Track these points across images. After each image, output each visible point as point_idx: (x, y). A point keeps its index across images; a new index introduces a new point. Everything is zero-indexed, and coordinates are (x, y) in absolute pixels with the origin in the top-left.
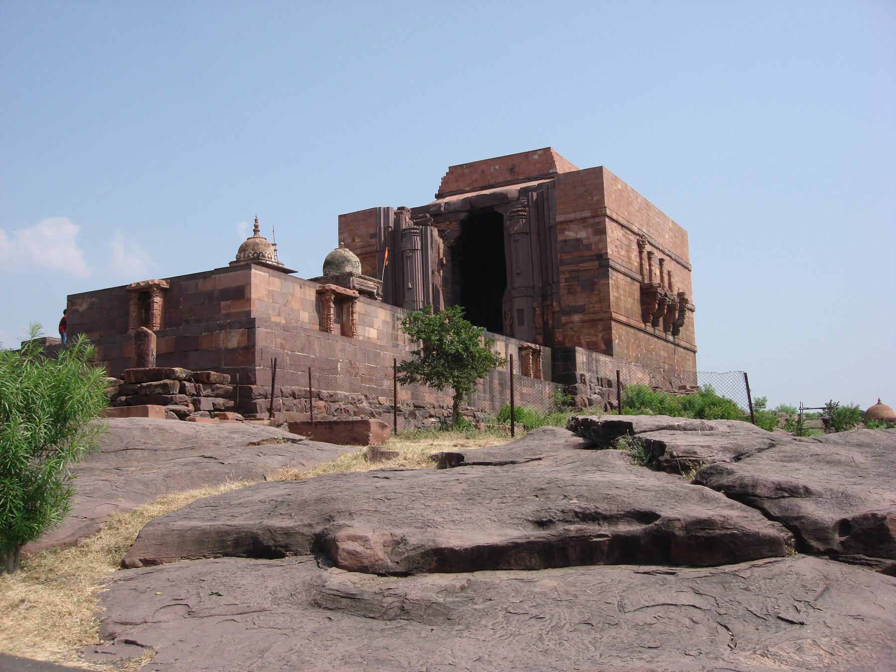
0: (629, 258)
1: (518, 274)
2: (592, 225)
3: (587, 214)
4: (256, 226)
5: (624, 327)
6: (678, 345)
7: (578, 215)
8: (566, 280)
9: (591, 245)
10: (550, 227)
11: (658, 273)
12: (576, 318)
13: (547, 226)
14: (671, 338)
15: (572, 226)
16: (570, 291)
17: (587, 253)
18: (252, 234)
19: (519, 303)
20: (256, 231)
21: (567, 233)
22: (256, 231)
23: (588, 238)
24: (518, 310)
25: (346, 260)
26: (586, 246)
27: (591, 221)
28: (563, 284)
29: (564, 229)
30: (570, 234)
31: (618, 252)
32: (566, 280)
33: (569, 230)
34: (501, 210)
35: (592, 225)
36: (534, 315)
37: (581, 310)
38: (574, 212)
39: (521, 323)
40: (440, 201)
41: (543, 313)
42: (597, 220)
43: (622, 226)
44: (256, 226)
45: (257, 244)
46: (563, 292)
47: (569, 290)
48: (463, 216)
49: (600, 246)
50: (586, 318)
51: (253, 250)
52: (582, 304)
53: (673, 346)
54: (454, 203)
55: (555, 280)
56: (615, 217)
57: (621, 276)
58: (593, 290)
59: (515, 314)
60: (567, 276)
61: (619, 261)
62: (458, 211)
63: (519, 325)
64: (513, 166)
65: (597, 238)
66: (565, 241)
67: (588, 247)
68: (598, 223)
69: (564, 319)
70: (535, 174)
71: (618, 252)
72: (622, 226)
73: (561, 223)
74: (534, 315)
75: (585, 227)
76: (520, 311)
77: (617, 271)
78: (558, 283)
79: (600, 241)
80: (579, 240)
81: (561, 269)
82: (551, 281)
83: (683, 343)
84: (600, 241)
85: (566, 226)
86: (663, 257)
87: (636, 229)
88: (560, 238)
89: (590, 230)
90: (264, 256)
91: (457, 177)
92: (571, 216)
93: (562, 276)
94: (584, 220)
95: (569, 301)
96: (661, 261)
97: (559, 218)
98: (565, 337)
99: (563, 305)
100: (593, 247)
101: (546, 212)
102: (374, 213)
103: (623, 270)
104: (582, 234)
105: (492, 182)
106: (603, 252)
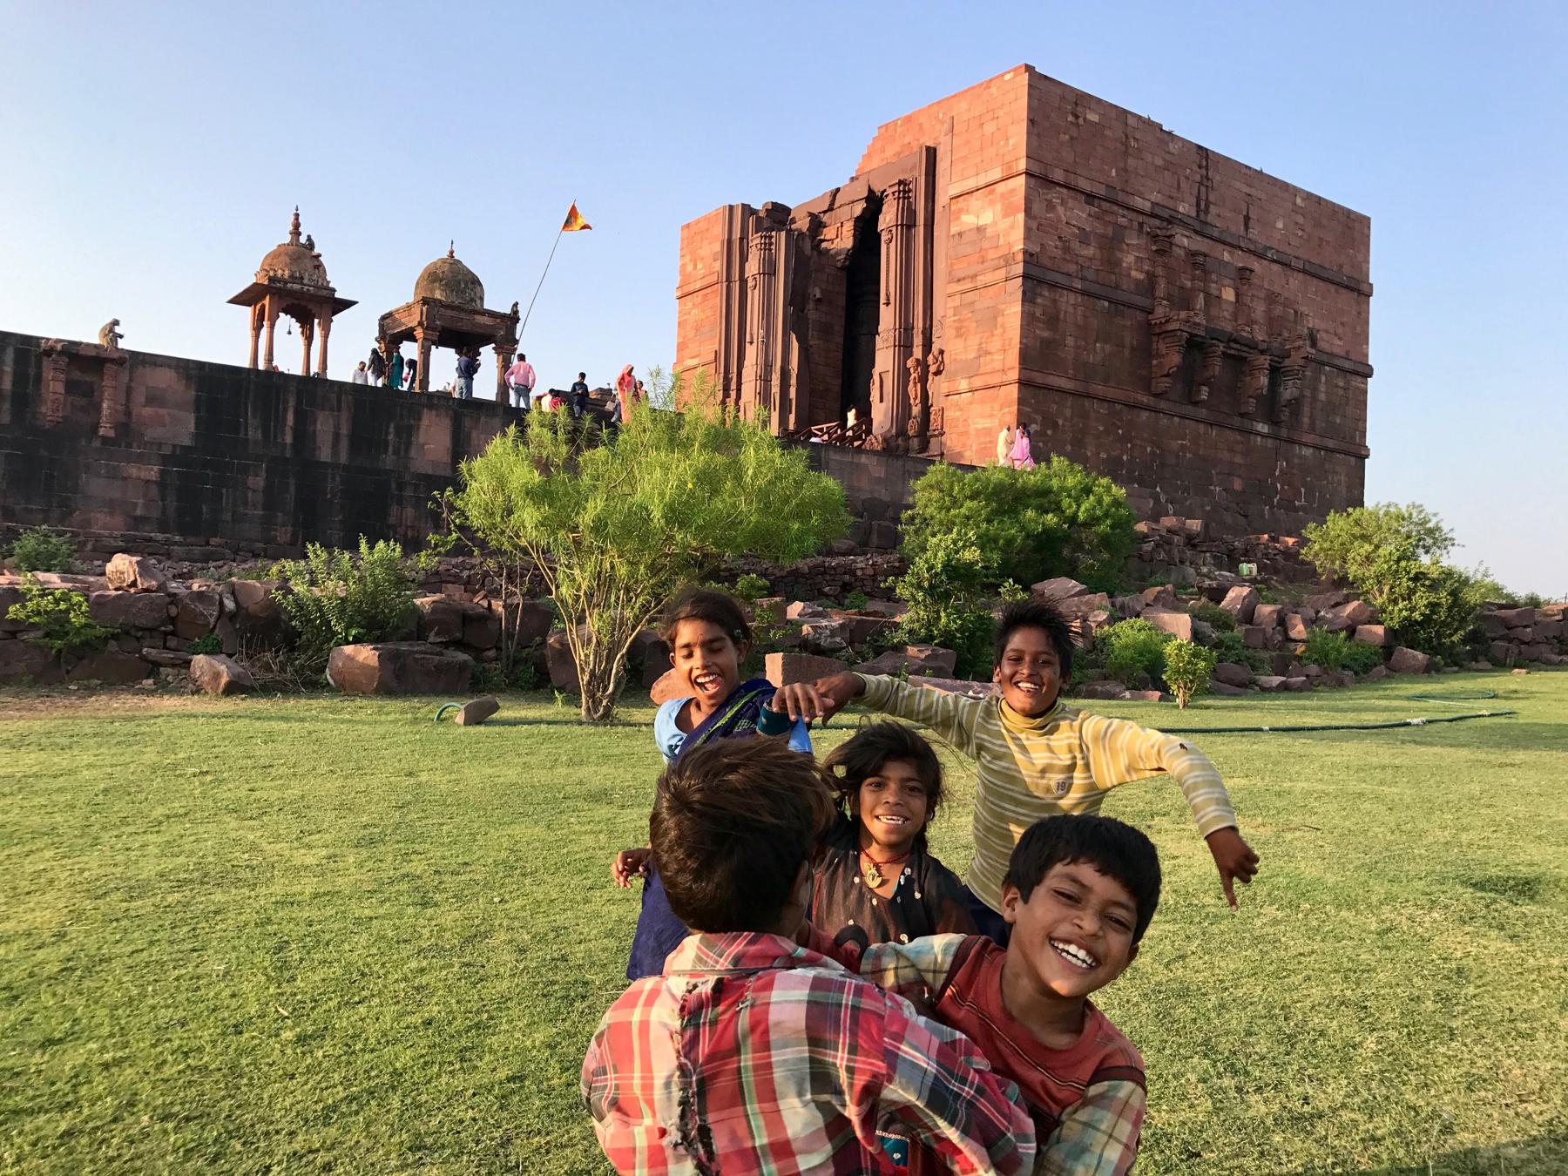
0: (1113, 264)
3: (996, 174)
4: (297, 226)
5: (1070, 401)
6: (1292, 441)
11: (1229, 295)
14: (1263, 428)
15: (975, 202)
18: (287, 239)
20: (296, 232)
21: (964, 218)
22: (296, 232)
23: (995, 223)
27: (1001, 188)
29: (960, 211)
30: (969, 220)
31: (1067, 250)
35: (1002, 195)
43: (1090, 198)
44: (297, 226)
47: (958, 329)
50: (978, 382)
53: (1270, 443)
56: (1058, 175)
57: (1072, 298)
61: (1072, 268)
71: (1067, 250)
72: (1090, 198)
75: (992, 203)
77: (1054, 286)
80: (980, 229)
83: (1307, 438)
86: (1256, 265)
87: (1147, 206)
88: (954, 229)
89: (999, 206)
92: (971, 184)
96: (1243, 275)
100: (1001, 241)
103: (1078, 285)
104: (986, 218)
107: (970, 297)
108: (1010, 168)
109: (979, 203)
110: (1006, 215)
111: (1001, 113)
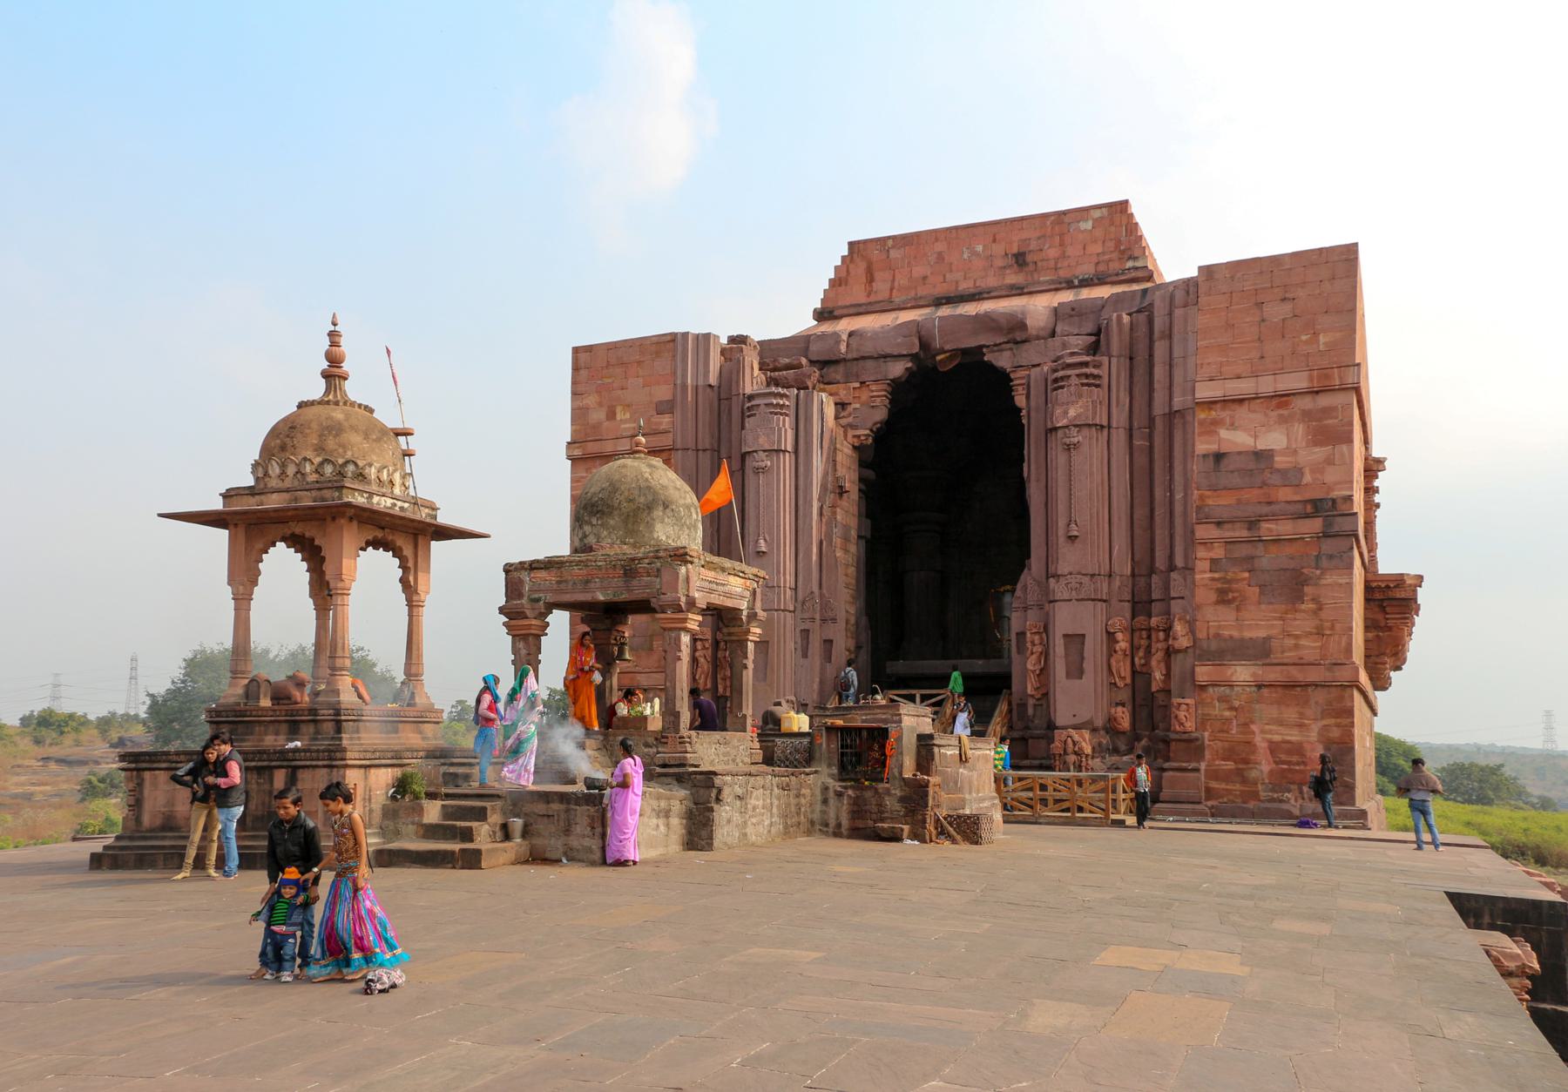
1: (1072, 539)
2: (1307, 415)
3: (1297, 381)
7: (1267, 385)
8: (1215, 564)
9: (1300, 471)
10: (1171, 415)
12: (1242, 673)
13: (1159, 408)
15: (1242, 412)
16: (1224, 597)
17: (1285, 494)
19: (1065, 619)
21: (1224, 433)
24: (1065, 636)
25: (650, 503)
26: (1283, 473)
27: (1306, 403)
28: (1203, 575)
29: (1216, 423)
30: (1236, 438)
32: (1215, 564)
33: (1232, 427)
34: (1003, 361)
35: (1307, 415)
36: (1111, 652)
37: (1259, 651)
38: (1255, 375)
39: (1075, 671)
40: (827, 328)
41: (1134, 649)
42: (1324, 401)
45: (336, 429)
46: (1205, 595)
47: (1222, 592)
48: (898, 369)
49: (1331, 476)
51: (320, 449)
52: (1262, 634)
54: (875, 335)
55: (1179, 562)
58: (1300, 598)
59: (1059, 648)
60: (1218, 552)
62: (885, 357)
63: (1069, 675)
64: (1026, 246)
65: (1320, 453)
66: (1219, 457)
67: (1292, 476)
68: (1328, 411)
69: (1203, 673)
70: (1087, 270)
73: (1211, 404)
74: (1111, 652)
75: (1283, 420)
76: (1075, 640)
78: (1189, 569)
79: (1330, 461)
81: (1202, 532)
82: (1160, 563)
84: (1330, 461)
85: (1225, 414)
88: (1203, 446)
89: (1299, 429)
90: (361, 476)
91: (868, 266)
92: (1245, 387)
93: (1201, 553)
94: (1281, 399)
95: (1218, 621)
97: (1205, 392)
98: (1202, 723)
99: (1201, 635)
100: (1308, 478)
101: (1159, 372)
102: (671, 343)
104: (1274, 440)
105: (965, 286)
106: (1335, 494)
107: (1244, 551)
108: (1327, 377)
109: (1258, 417)
110: (1316, 443)
111: (1301, 293)
